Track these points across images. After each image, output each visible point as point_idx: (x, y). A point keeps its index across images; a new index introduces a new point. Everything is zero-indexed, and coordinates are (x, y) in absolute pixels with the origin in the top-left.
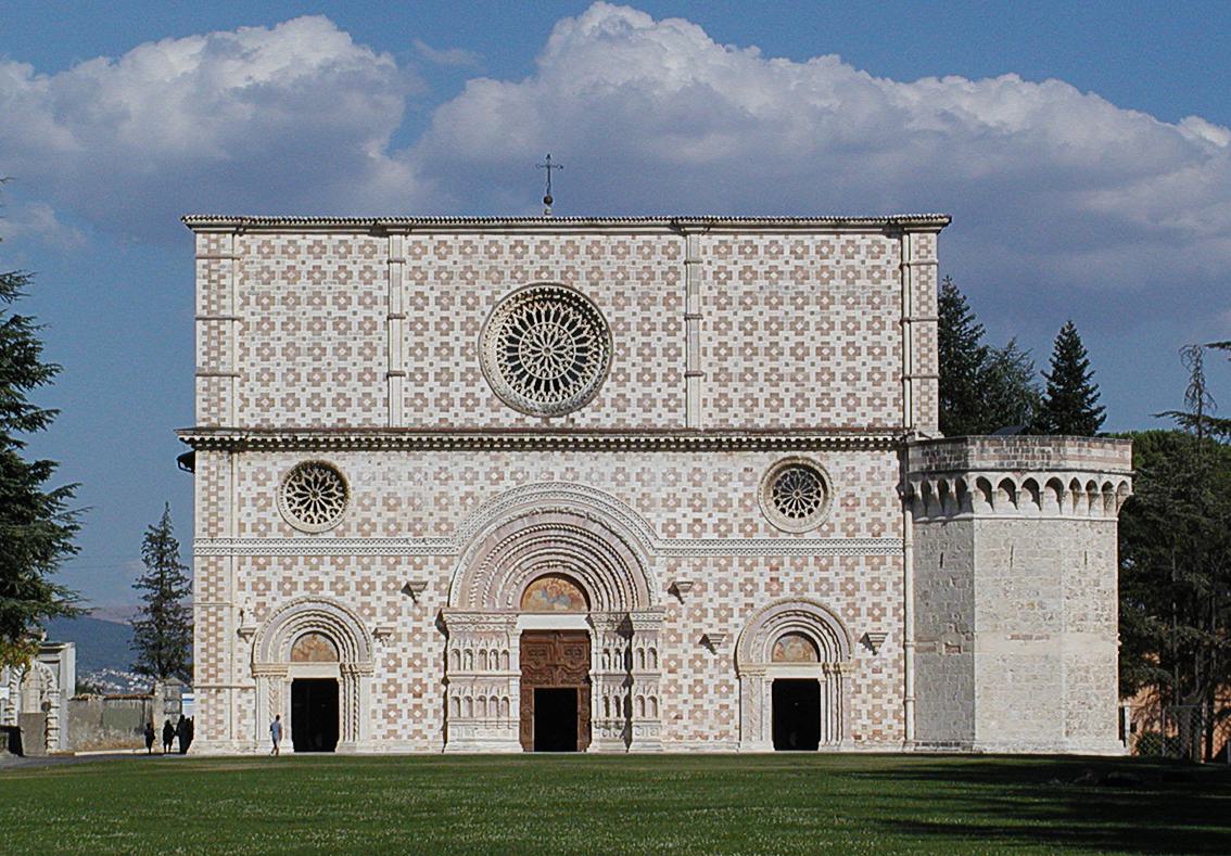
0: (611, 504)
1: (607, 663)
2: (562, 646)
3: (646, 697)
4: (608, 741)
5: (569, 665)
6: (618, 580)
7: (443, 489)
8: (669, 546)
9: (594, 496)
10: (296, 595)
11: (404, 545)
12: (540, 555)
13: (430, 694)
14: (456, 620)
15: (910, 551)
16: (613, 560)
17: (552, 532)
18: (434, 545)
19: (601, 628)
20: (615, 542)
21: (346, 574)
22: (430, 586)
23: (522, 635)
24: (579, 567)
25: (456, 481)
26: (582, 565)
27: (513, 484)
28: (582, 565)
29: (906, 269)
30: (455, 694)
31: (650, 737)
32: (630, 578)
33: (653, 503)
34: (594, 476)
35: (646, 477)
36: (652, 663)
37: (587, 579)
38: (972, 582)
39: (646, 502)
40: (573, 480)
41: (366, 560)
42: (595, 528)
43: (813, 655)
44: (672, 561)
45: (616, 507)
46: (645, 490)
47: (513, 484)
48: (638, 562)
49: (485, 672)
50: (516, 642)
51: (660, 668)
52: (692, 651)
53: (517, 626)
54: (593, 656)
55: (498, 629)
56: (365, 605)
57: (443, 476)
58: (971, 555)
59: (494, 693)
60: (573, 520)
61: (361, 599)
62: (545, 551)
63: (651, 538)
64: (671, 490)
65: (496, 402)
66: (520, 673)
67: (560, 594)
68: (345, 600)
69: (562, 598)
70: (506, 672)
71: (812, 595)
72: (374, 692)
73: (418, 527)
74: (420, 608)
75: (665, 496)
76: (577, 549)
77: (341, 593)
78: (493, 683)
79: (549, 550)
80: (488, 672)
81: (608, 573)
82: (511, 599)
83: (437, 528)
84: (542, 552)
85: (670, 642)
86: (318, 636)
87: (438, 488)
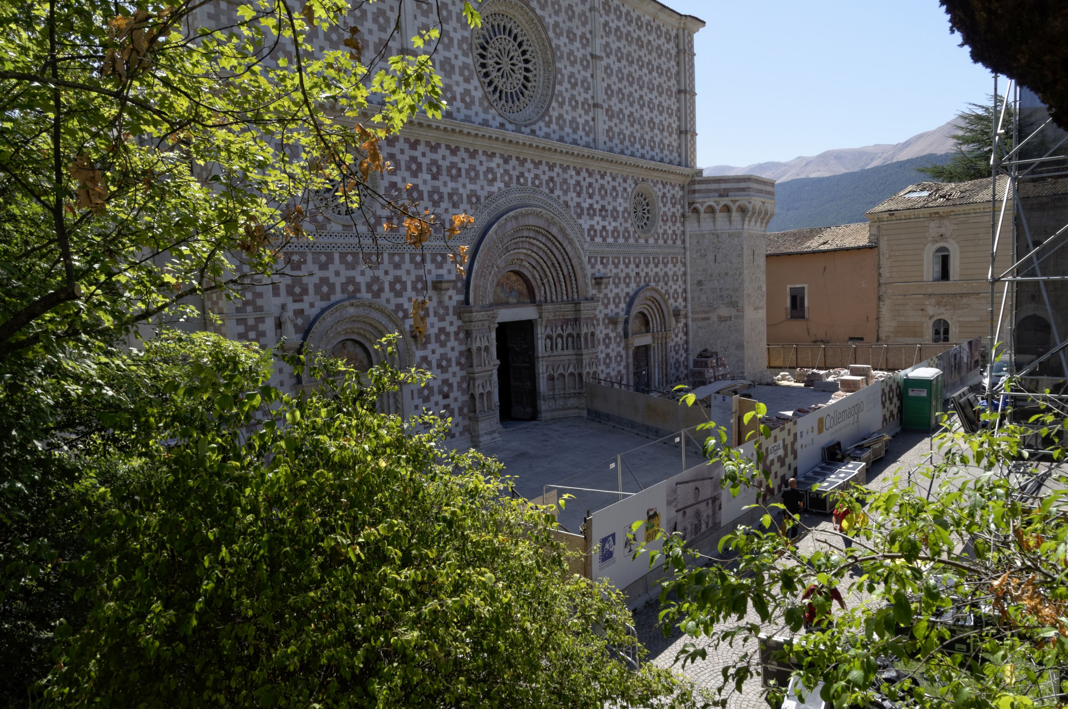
4: (553, 410)
10: (334, 298)
13: (455, 394)
15: (688, 254)
21: (380, 273)
26: (534, 263)
27: (502, 185)
29: (682, 55)
38: (741, 274)
41: (397, 258)
42: (554, 231)
43: (643, 329)
52: (605, 332)
56: (399, 307)
58: (741, 256)
60: (541, 223)
61: (395, 301)
65: (486, 104)
66: (498, 362)
68: (382, 301)
69: (514, 293)
71: (653, 284)
72: (413, 398)
77: (377, 295)
81: (553, 270)
86: (349, 343)
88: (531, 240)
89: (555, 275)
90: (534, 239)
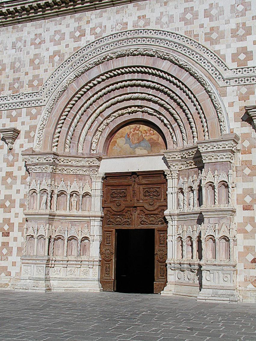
0: (181, 42)
1: (182, 204)
2: (141, 187)
3: (217, 236)
5: (146, 206)
6: (189, 116)
7: (37, 51)
8: (239, 75)
9: (164, 37)
11: (6, 102)
12: (118, 102)
14: (35, 161)
16: (184, 96)
17: (126, 77)
18: (27, 99)
19: (176, 168)
20: (184, 76)
22: (22, 135)
23: (103, 179)
24: (156, 111)
25: (48, 44)
26: (157, 107)
28: (157, 107)
30: (30, 232)
31: (222, 283)
32: (201, 110)
33: (222, 36)
34: (165, 19)
35: (214, 12)
36: (224, 198)
37: (162, 121)
39: (214, 36)
40: (144, 27)
42: (165, 66)
44: (244, 90)
45: (185, 44)
46: (213, 24)
47: (92, 38)
48: (208, 92)
49: (63, 212)
50: (98, 185)
51: (234, 204)
53: (100, 170)
54: (169, 197)
55: (81, 173)
57: (37, 41)
59: (72, 233)
62: (123, 97)
63: (221, 69)
64: (240, 20)
67: (141, 140)
69: (143, 144)
70: (86, 213)
73: (16, 85)
74: (13, 155)
75: (234, 27)
76: (151, 91)
78: (73, 223)
79: (127, 96)
80: (67, 212)
82: (94, 145)
83: (31, 85)
84: (120, 98)
85: (244, 175)
87: (33, 51)
88: (139, 82)
89: (183, 115)
90: (143, 80)
